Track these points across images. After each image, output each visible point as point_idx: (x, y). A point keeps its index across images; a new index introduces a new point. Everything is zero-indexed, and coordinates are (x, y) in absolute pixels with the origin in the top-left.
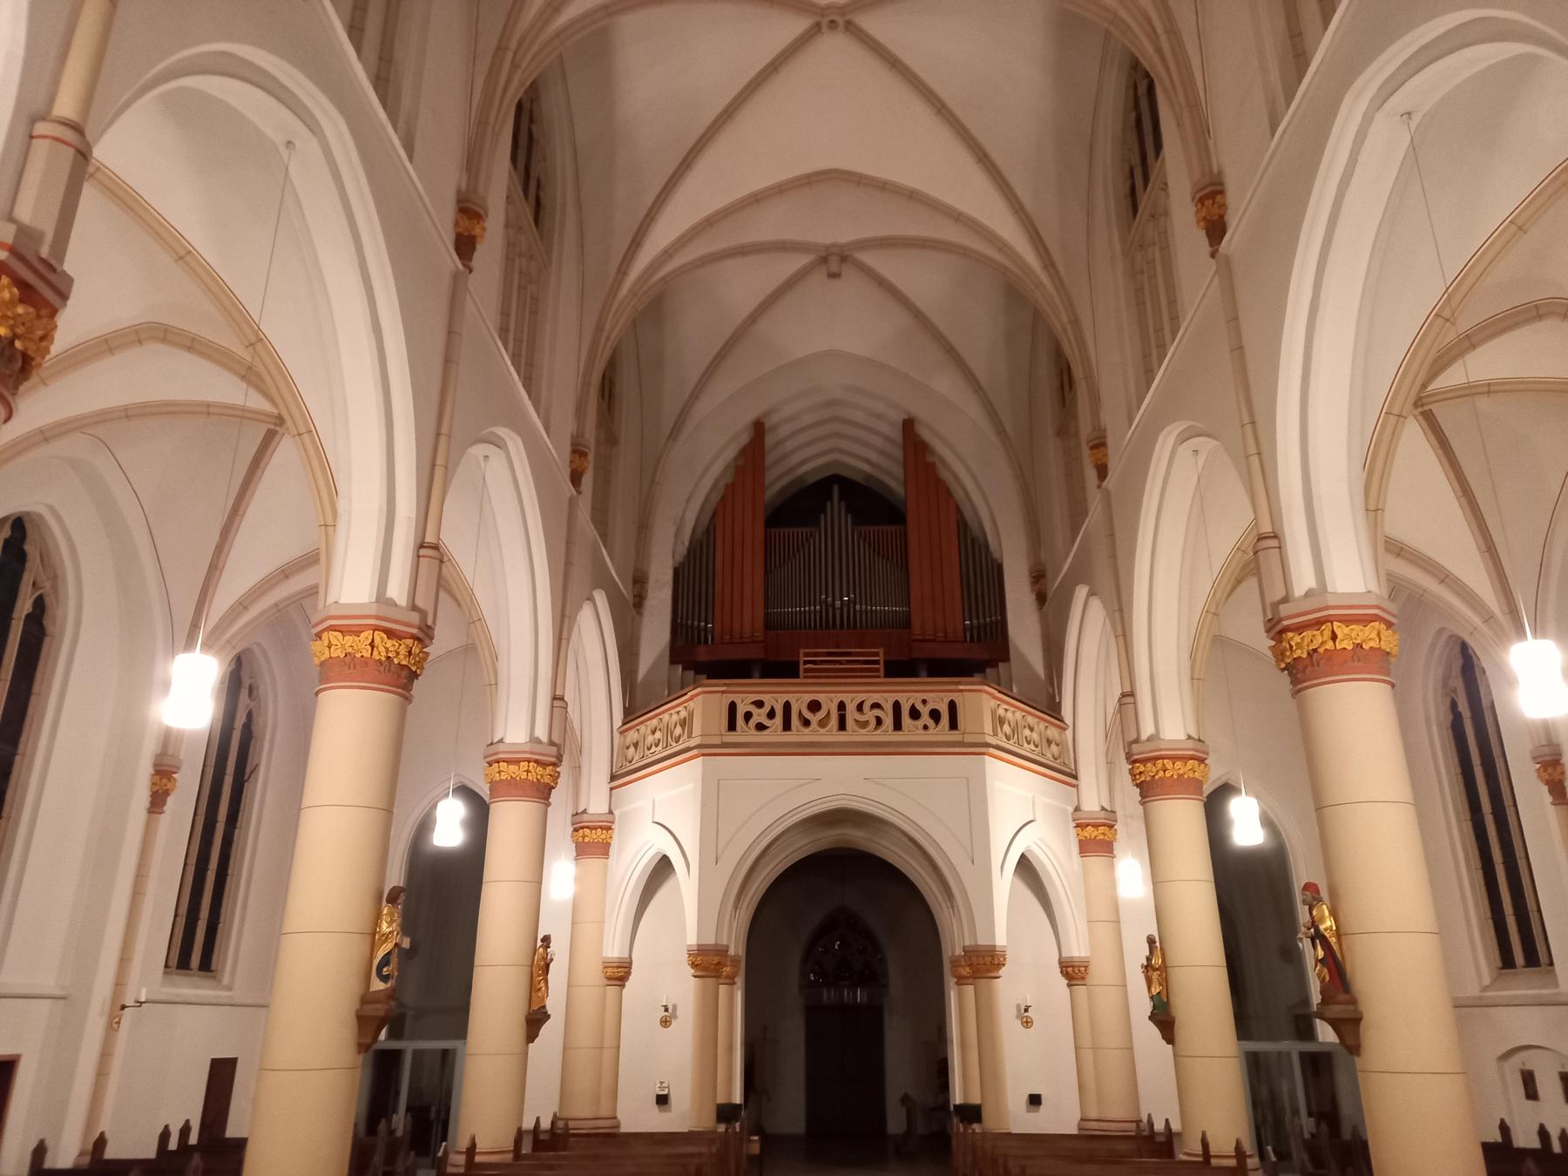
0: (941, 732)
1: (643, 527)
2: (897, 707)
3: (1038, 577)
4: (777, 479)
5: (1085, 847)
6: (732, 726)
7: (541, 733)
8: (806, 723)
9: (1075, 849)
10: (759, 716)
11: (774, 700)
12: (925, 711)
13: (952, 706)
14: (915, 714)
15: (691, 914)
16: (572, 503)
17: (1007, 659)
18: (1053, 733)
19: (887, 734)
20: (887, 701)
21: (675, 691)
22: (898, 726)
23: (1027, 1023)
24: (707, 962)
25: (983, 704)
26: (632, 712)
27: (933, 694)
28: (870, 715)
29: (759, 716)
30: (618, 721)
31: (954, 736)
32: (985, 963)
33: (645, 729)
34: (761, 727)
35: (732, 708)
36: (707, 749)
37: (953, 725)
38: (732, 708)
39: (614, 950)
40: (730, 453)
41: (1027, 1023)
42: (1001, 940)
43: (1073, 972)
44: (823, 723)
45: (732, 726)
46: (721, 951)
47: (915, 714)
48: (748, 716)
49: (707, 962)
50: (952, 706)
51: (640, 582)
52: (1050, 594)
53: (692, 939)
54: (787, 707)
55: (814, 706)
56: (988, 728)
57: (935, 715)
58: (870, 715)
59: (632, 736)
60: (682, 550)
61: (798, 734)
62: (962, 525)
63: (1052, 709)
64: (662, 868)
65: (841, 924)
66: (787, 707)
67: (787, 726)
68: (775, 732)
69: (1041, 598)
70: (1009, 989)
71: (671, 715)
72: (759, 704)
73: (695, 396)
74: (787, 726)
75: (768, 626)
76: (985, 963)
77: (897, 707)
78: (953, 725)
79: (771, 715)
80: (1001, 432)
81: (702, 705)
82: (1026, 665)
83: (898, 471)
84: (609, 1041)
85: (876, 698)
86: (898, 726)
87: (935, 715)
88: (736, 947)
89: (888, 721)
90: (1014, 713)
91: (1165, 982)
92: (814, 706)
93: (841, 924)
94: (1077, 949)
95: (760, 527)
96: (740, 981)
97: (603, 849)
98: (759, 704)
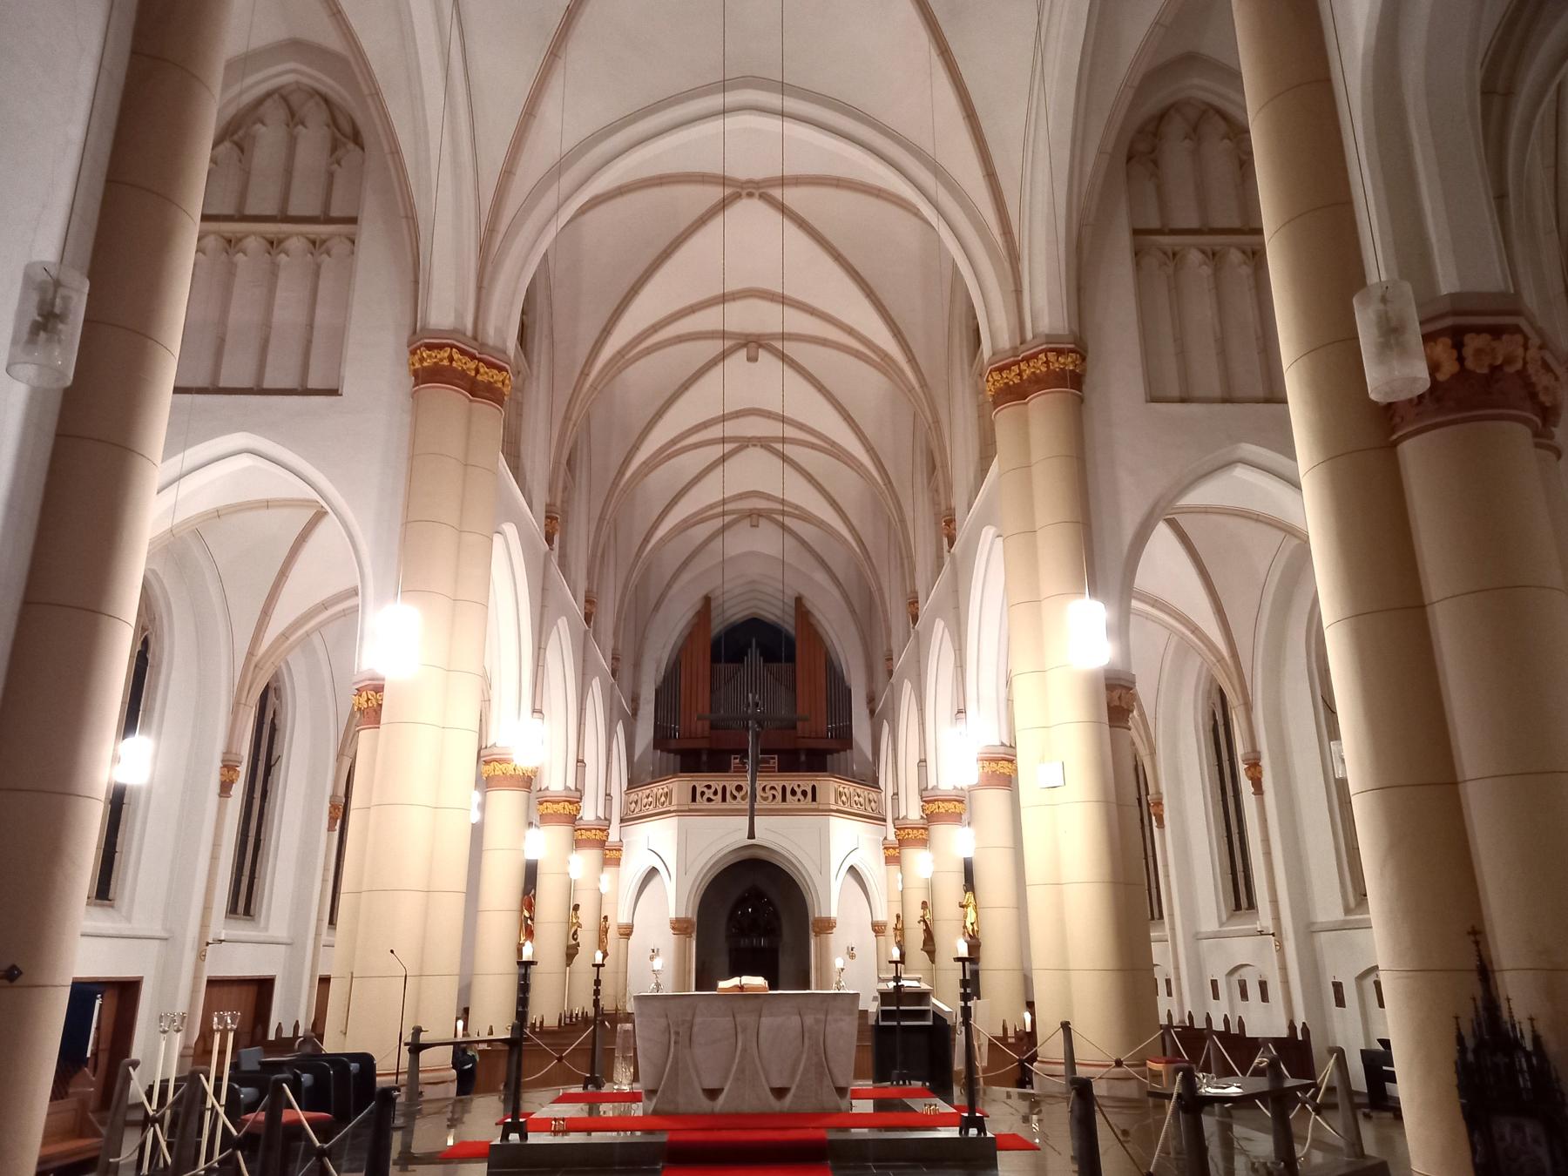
0: (807, 803)
1: (637, 666)
2: (784, 788)
3: (871, 700)
4: (717, 626)
5: (889, 860)
6: (694, 800)
7: (571, 784)
8: (735, 798)
9: (883, 861)
10: (709, 794)
11: (717, 784)
12: (799, 791)
13: (814, 788)
14: (793, 793)
15: (671, 900)
16: (586, 632)
17: (851, 747)
18: (873, 796)
19: (778, 804)
20: (779, 785)
21: (659, 775)
22: (784, 800)
23: (852, 957)
24: (680, 927)
25: (831, 787)
26: (633, 783)
27: (804, 782)
28: (769, 793)
29: (709, 794)
30: (625, 787)
31: (814, 805)
32: (827, 926)
33: (642, 794)
34: (709, 800)
35: (694, 788)
36: (680, 812)
37: (814, 799)
38: (694, 788)
39: (624, 919)
40: (690, 614)
41: (852, 957)
42: (834, 914)
43: (878, 929)
44: (743, 798)
45: (694, 800)
46: (686, 920)
47: (793, 793)
48: (703, 793)
49: (680, 927)
50: (814, 788)
51: (635, 701)
52: (896, 669)
53: (673, 915)
54: (724, 788)
55: (739, 788)
56: (832, 801)
57: (804, 793)
58: (769, 793)
59: (633, 797)
60: (660, 678)
61: (730, 804)
62: (827, 653)
63: (873, 782)
64: (653, 871)
65: (755, 896)
66: (724, 788)
67: (724, 800)
68: (717, 803)
69: (872, 712)
70: (838, 941)
71: (659, 789)
72: (709, 787)
73: (669, 586)
74: (724, 800)
75: (712, 727)
76: (827, 926)
77: (784, 788)
78: (814, 799)
79: (715, 793)
80: (853, 612)
81: (677, 787)
82: (861, 752)
83: (792, 621)
84: (622, 969)
85: (773, 784)
86: (784, 800)
87: (804, 793)
88: (692, 914)
89: (779, 797)
90: (848, 788)
91: (902, 935)
92: (739, 788)
93: (755, 896)
94: (881, 916)
95: (708, 664)
96: (694, 935)
97: (617, 862)
98: (709, 787)
